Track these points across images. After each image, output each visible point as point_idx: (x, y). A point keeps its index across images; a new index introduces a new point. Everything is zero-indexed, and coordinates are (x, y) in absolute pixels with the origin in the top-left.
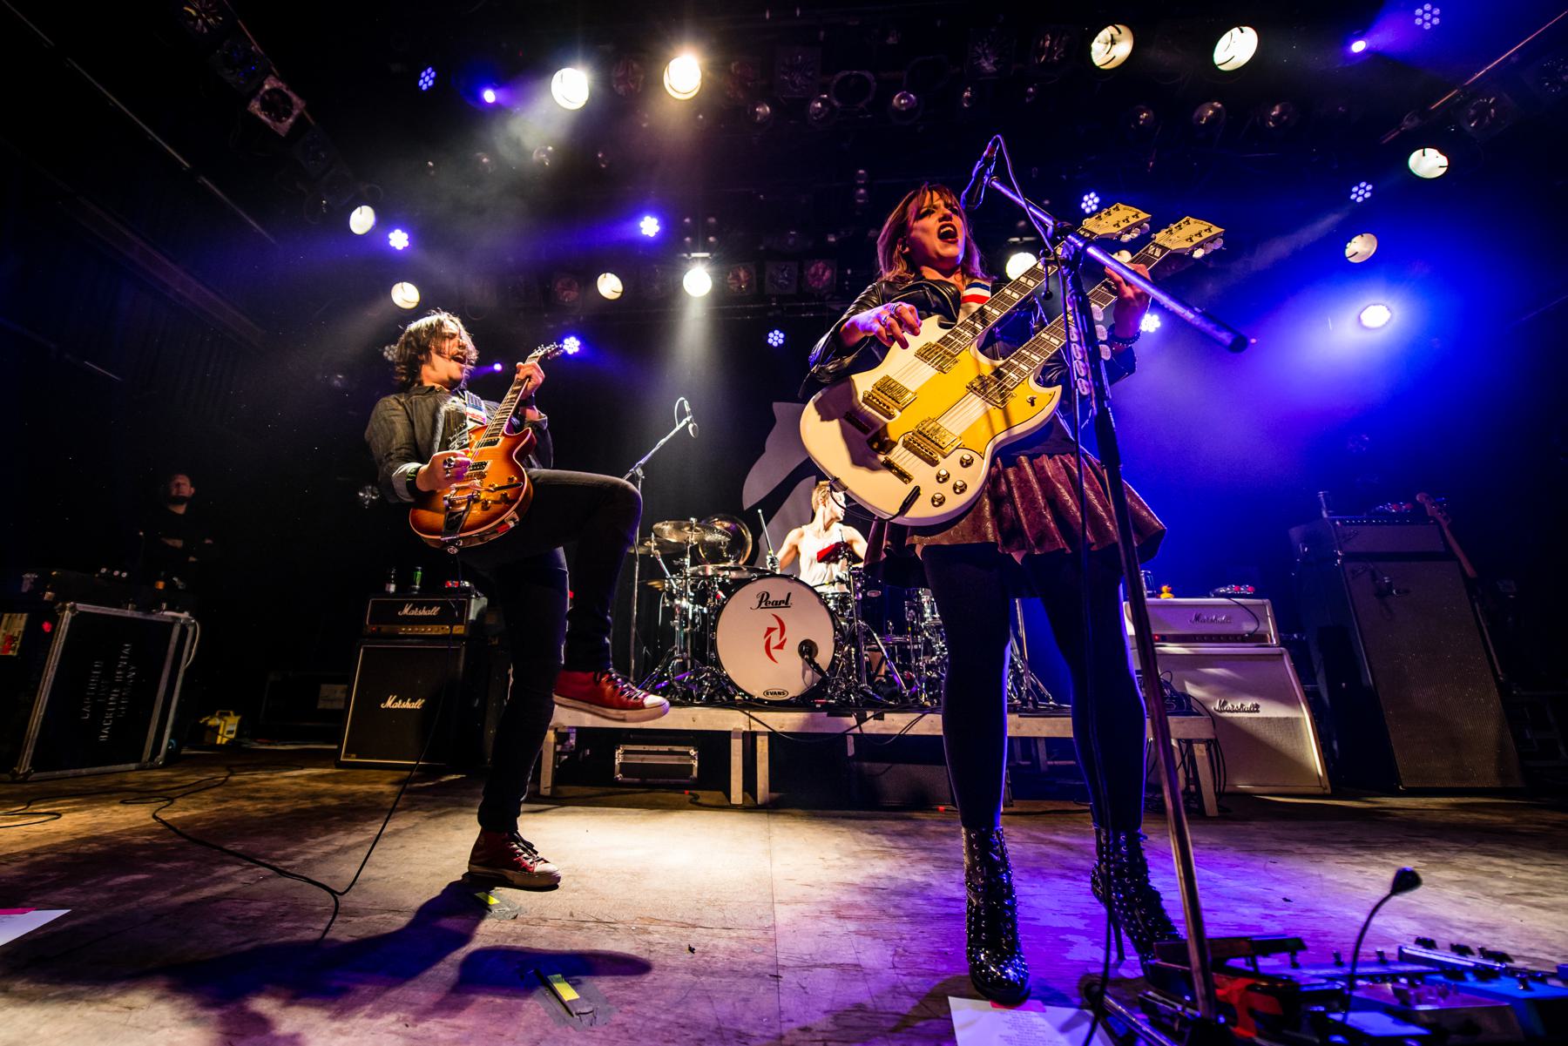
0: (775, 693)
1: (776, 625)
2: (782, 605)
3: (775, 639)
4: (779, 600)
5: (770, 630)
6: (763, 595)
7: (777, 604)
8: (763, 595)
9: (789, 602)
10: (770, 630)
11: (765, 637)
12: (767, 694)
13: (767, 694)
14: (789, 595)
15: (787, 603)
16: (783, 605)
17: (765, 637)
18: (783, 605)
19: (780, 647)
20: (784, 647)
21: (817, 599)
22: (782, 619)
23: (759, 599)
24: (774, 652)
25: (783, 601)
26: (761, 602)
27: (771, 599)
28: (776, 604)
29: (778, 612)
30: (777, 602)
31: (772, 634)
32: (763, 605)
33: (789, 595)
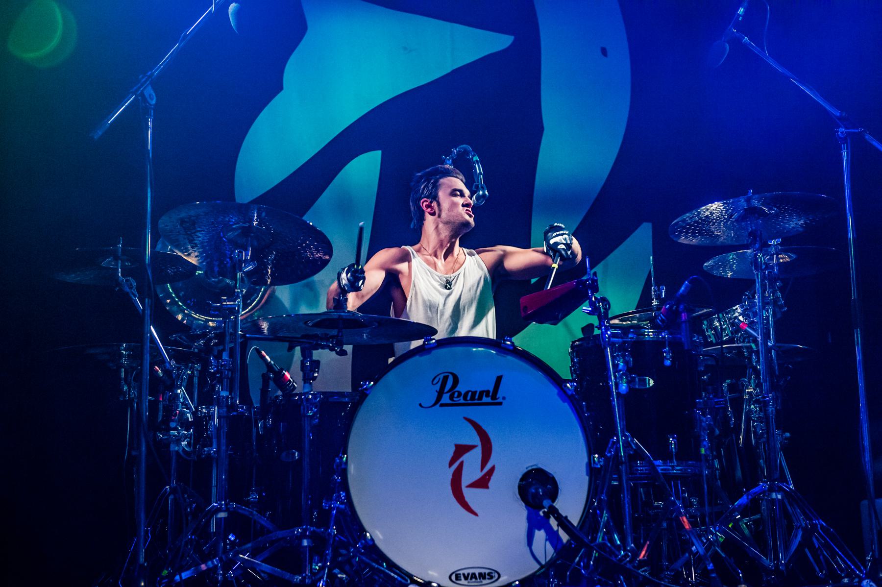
0: (473, 576)
1: (474, 439)
2: (485, 399)
3: (472, 470)
4: (479, 389)
5: (461, 450)
6: (445, 379)
7: (474, 399)
8: (445, 379)
9: (500, 394)
10: (461, 450)
11: (451, 464)
12: (458, 577)
13: (458, 577)
14: (499, 379)
15: (494, 397)
16: (489, 400)
17: (451, 464)
18: (489, 400)
19: (482, 483)
20: (490, 484)
21: (555, 391)
22: (484, 427)
23: (438, 387)
24: (470, 495)
25: (488, 392)
26: (440, 394)
27: (462, 388)
28: (473, 398)
29: (476, 413)
30: (474, 393)
31: (466, 458)
32: (446, 399)
33: (499, 379)
